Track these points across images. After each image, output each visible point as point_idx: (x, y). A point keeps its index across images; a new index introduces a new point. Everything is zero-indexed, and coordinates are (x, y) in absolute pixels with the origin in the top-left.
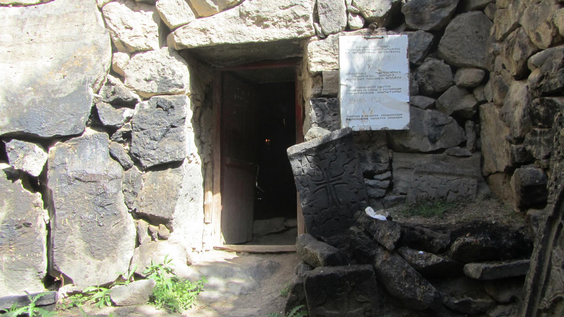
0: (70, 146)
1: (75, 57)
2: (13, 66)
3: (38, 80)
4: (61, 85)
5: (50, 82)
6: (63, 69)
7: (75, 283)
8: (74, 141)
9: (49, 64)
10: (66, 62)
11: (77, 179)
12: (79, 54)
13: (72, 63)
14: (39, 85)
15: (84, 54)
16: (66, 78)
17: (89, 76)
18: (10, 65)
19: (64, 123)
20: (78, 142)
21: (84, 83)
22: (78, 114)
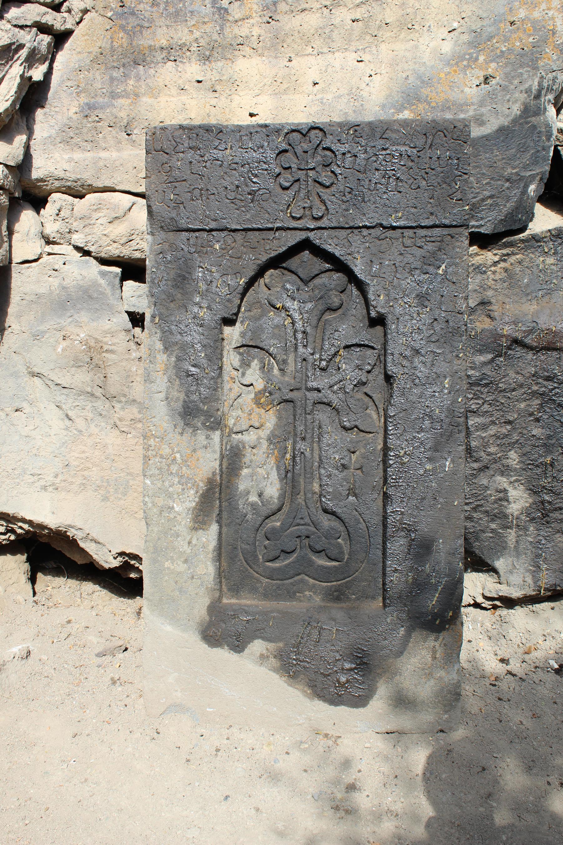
0: (496, 259)
1: (512, 23)
2: (366, 57)
3: (425, 91)
4: (482, 104)
5: (455, 95)
6: (482, 58)
7: (503, 579)
8: (506, 245)
9: (447, 48)
10: (490, 38)
11: (516, 341)
12: (522, 13)
13: (507, 40)
14: (429, 103)
15: (536, 15)
16: (493, 82)
17: (550, 76)
18: (356, 56)
19: (489, 201)
20: (515, 250)
21: (538, 96)
22: (522, 178)
